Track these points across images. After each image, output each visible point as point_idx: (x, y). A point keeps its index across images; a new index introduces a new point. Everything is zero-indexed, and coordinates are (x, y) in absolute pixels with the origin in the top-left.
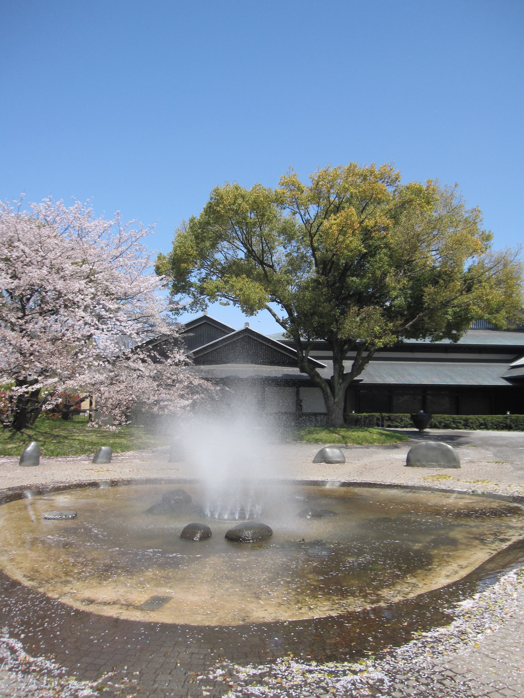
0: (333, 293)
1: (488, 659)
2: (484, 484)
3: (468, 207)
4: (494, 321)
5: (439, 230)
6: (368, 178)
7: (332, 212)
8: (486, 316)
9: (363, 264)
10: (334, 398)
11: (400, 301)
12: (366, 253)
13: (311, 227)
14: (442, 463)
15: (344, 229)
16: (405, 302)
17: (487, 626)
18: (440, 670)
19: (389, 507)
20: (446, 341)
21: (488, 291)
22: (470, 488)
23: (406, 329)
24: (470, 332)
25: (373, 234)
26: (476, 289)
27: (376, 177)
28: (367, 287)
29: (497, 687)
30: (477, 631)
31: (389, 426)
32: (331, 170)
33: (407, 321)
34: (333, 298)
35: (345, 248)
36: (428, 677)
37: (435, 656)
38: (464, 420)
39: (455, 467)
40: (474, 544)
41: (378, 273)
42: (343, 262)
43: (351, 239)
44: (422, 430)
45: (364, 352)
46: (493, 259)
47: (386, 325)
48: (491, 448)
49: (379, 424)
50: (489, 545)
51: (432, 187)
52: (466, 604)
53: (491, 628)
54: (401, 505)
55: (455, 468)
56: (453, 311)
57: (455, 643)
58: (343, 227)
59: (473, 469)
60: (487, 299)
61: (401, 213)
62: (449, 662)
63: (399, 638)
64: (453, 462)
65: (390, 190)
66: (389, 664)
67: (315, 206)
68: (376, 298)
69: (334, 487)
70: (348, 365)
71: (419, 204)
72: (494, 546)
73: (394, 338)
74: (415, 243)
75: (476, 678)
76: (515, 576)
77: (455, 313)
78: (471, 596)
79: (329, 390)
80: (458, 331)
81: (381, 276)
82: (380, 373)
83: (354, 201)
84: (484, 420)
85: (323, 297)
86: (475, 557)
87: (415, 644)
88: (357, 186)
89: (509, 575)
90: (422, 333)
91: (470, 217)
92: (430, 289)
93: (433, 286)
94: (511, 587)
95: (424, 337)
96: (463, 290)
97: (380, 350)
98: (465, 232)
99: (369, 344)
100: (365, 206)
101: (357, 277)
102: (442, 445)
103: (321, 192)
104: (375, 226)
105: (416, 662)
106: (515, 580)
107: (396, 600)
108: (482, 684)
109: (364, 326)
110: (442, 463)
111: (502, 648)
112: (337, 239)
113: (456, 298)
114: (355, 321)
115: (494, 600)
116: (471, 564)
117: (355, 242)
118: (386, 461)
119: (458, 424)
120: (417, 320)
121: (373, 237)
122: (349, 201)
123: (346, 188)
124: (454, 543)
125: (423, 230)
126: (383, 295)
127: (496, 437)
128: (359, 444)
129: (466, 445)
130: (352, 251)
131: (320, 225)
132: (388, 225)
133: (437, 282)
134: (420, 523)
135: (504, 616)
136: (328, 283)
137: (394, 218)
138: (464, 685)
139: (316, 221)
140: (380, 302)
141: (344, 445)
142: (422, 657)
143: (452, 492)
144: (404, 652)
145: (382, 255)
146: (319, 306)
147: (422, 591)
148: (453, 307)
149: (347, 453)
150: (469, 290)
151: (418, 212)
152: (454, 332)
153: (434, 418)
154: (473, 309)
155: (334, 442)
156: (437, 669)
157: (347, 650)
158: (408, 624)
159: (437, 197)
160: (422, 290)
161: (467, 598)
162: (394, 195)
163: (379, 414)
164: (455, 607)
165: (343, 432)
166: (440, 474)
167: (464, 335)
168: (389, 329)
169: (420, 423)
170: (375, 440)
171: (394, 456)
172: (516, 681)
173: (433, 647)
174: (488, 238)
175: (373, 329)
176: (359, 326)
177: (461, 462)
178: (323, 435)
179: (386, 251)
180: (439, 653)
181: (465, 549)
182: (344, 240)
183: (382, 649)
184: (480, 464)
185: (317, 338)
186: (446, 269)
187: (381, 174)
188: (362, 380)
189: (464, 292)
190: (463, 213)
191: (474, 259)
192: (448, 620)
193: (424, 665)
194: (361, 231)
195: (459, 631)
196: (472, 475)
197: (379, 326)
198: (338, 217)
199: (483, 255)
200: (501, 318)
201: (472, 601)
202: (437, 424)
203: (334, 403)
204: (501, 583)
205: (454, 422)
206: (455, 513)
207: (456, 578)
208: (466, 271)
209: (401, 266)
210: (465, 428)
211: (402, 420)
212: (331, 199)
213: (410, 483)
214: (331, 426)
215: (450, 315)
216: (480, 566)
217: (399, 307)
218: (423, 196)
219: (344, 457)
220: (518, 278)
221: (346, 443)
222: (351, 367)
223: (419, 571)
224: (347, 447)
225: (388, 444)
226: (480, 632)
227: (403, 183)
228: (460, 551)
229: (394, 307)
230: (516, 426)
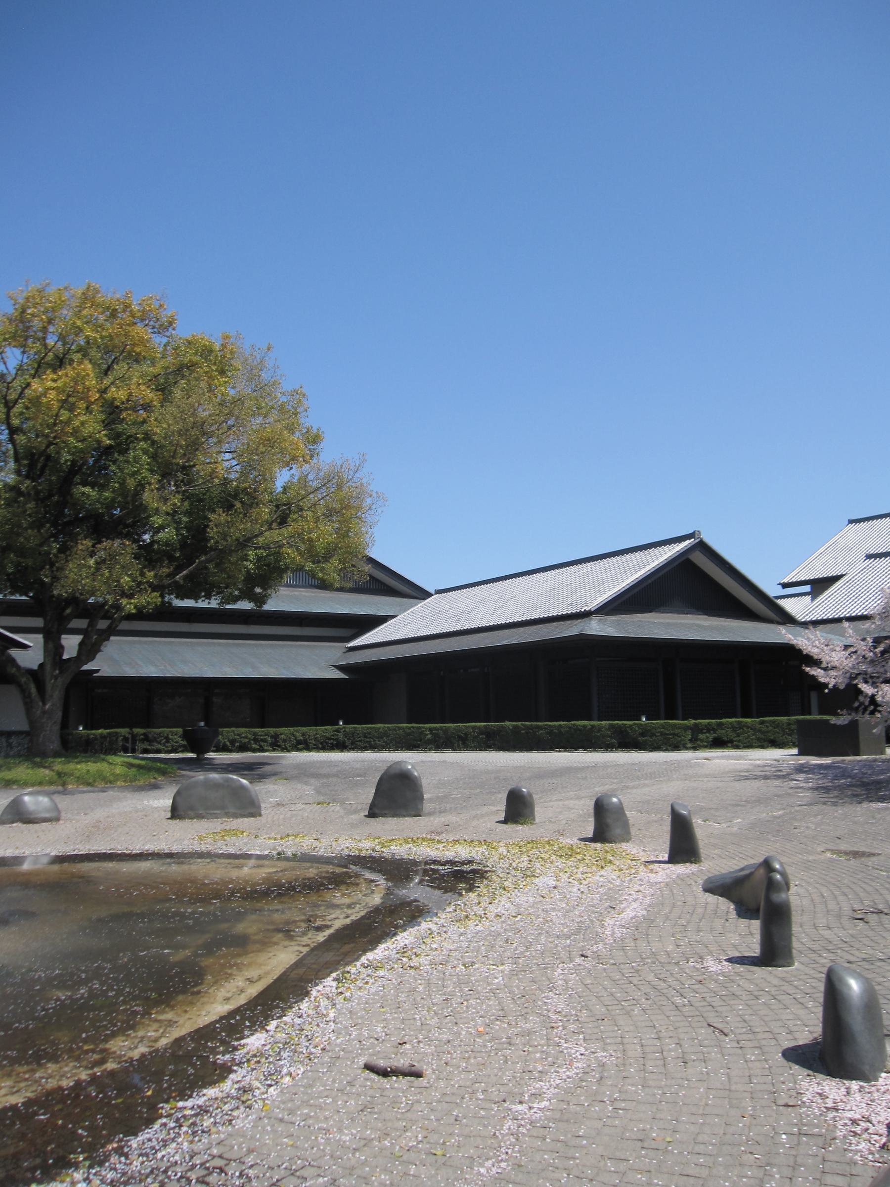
0: (46, 513)
1: (283, 1125)
2: (297, 840)
3: (287, 386)
4: (320, 575)
5: (237, 418)
6: (119, 315)
7: (49, 365)
8: (309, 566)
9: (105, 464)
10: (44, 704)
11: (168, 534)
12: (111, 445)
13: (8, 388)
14: (232, 810)
15: (70, 399)
16: (177, 535)
17: (285, 1071)
18: (203, 1161)
19: (131, 894)
20: (245, 605)
21: (312, 525)
22: (274, 849)
23: (176, 582)
24: (283, 591)
25: (124, 415)
26: (294, 520)
27: (133, 317)
28: (110, 506)
29: (294, 1167)
30: (269, 1082)
31: (146, 751)
32: (52, 290)
33: (178, 569)
34: (47, 522)
35: (71, 434)
36: (181, 1177)
37: (197, 1139)
38: (272, 737)
39: (252, 815)
40: (275, 939)
41: (131, 483)
42: (69, 457)
43: (82, 418)
44: (201, 756)
45: (102, 621)
46: (322, 474)
47: (142, 574)
48: (312, 781)
49: (128, 747)
50: (298, 938)
51: (229, 347)
52: (255, 1041)
53: (290, 1074)
54: (153, 888)
55: (253, 816)
56: (256, 555)
57: (231, 1110)
58: (69, 396)
59: (282, 816)
60: (309, 538)
61: (175, 383)
62: (219, 1144)
63: (135, 1118)
64: (249, 807)
65: (158, 341)
66: (115, 1169)
67: (17, 352)
68: (127, 526)
69: (38, 866)
70: (71, 644)
71: (206, 372)
72: (305, 940)
73: (156, 597)
74: (196, 436)
75: (262, 1161)
76: (334, 984)
77: (259, 559)
78: (263, 1027)
79: (33, 690)
80: (265, 589)
81: (135, 489)
82: (129, 658)
83: (93, 352)
84: (303, 735)
85: (25, 519)
86: (274, 962)
87: (165, 1125)
88: (98, 327)
89: (325, 984)
90: (204, 590)
91: (288, 402)
92: (218, 517)
93: (224, 512)
94: (326, 1002)
95: (208, 596)
96: (273, 522)
97: (130, 617)
98: (279, 426)
99: (112, 606)
100: (113, 362)
101: (93, 488)
102: (233, 779)
103: (28, 328)
104: (128, 400)
105: (163, 1156)
106: (334, 990)
107: (136, 1054)
108: (269, 1167)
109: (102, 575)
110: (232, 810)
111: (306, 1103)
112: (57, 415)
113: (261, 533)
114: (85, 566)
115: (299, 1027)
116: (267, 973)
117: (90, 425)
118: (137, 812)
119: (262, 744)
120: (194, 569)
121: (124, 419)
122: (83, 351)
123: (78, 327)
124: (241, 943)
125: (210, 415)
126: (138, 521)
127: (322, 763)
128: (89, 784)
129: (273, 778)
130: (85, 440)
131: (26, 388)
132: (152, 401)
133: (231, 507)
134: (183, 916)
135: (313, 1050)
136: (38, 492)
137: (162, 390)
138: (241, 1175)
139: (19, 378)
140: (133, 534)
141: (60, 788)
142: (174, 1145)
143: (248, 857)
144: (143, 1143)
145: (139, 452)
146: (19, 535)
147: (183, 1032)
148: (256, 548)
149: (63, 802)
150: (283, 521)
151: (203, 385)
152: (258, 590)
153: (222, 735)
154: (288, 554)
155: (40, 784)
156: (197, 1161)
157: (38, 1161)
158: (153, 1092)
159: (237, 363)
160: (206, 518)
161: (256, 1030)
162: (165, 350)
163: (128, 730)
164: (235, 1049)
165: (59, 765)
166: (228, 828)
167: (273, 595)
168: (147, 582)
169: (198, 743)
170: (117, 777)
171: (151, 802)
172: (323, 1150)
173: (194, 1124)
174: (314, 439)
175: (118, 581)
176: (93, 575)
177: (263, 805)
178: (22, 771)
179: (145, 446)
180: (203, 1132)
181: (259, 951)
182: (69, 420)
183: (103, 1146)
184: (293, 807)
185: (12, 594)
186: (247, 485)
187: (143, 311)
188: (97, 671)
189: (275, 525)
190: (279, 395)
191: (292, 472)
192: (225, 1071)
193: (177, 1157)
194: (102, 406)
195: (239, 1089)
196: (279, 826)
197: (129, 576)
198: (60, 378)
199: (306, 467)
200: (331, 570)
201: (264, 1035)
202: (228, 744)
203: (44, 712)
204: (312, 999)
205: (256, 740)
206: (247, 893)
207: (242, 1000)
208: (280, 489)
209: (170, 474)
210: (274, 750)
211: (168, 740)
212: (48, 341)
213: (176, 848)
214: (36, 756)
215: (251, 562)
216: (281, 975)
217: (167, 544)
218: (211, 361)
219: (59, 811)
220: (359, 508)
221: (64, 784)
222: (77, 648)
223: (180, 998)
224: (65, 792)
225: (142, 783)
226: (273, 1083)
227: (183, 331)
228: (252, 955)
229: (158, 543)
230: (352, 743)
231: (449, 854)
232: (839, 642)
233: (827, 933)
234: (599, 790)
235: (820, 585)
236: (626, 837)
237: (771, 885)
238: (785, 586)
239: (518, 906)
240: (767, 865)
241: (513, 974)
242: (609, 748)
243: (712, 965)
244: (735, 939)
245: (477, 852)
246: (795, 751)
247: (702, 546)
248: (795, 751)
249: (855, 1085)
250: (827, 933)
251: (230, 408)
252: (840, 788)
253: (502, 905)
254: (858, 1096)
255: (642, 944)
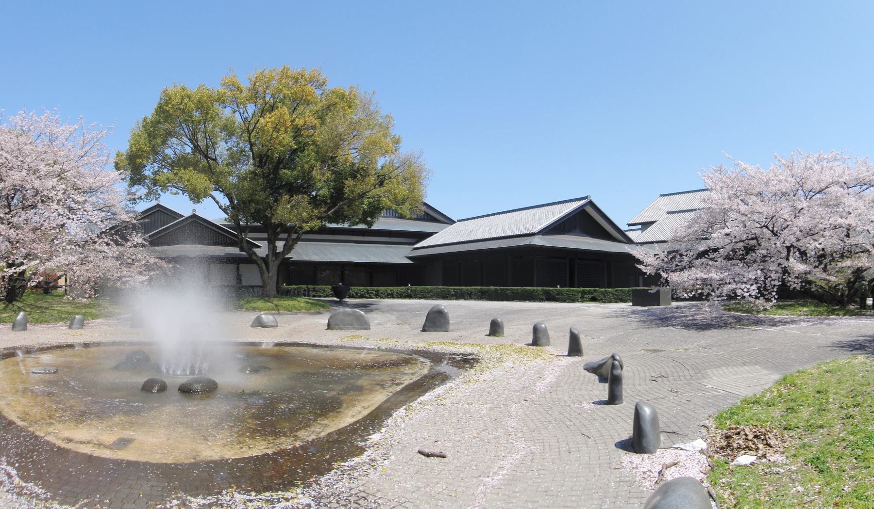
3: (383, 113)
7: (267, 110)
8: (394, 207)
11: (324, 192)
20: (362, 226)
24: (381, 219)
27: (306, 80)
28: (297, 179)
31: (314, 296)
32: (267, 72)
39: (366, 329)
41: (307, 166)
43: (283, 135)
45: (294, 234)
47: (312, 211)
49: (306, 294)
65: (318, 93)
70: (280, 245)
72: (391, 389)
77: (370, 203)
82: (307, 252)
83: (287, 101)
86: (375, 399)
92: (349, 182)
95: (343, 222)
97: (307, 232)
98: (379, 134)
117: (287, 139)
122: (282, 102)
124: (360, 389)
145: (310, 151)
149: (279, 318)
150: (381, 184)
152: (369, 219)
160: (343, 183)
165: (276, 301)
169: (340, 294)
174: (397, 141)
178: (260, 304)
182: (277, 137)
199: (393, 156)
211: (324, 291)
213: (329, 344)
220: (420, 177)
224: (279, 314)
227: (329, 87)
231: (462, 351)
232: (652, 253)
233: (639, 388)
234: (535, 321)
235: (646, 225)
236: (548, 344)
237: (613, 367)
238: (630, 225)
239: (494, 376)
240: (613, 357)
241: (491, 409)
242: (541, 300)
243: (586, 406)
244: (597, 393)
245: (475, 350)
246: (631, 304)
247: (591, 203)
248: (631, 304)
249: (646, 456)
250: (639, 388)
251: (354, 127)
252: (651, 321)
253: (487, 375)
254: (647, 461)
255: (554, 395)
